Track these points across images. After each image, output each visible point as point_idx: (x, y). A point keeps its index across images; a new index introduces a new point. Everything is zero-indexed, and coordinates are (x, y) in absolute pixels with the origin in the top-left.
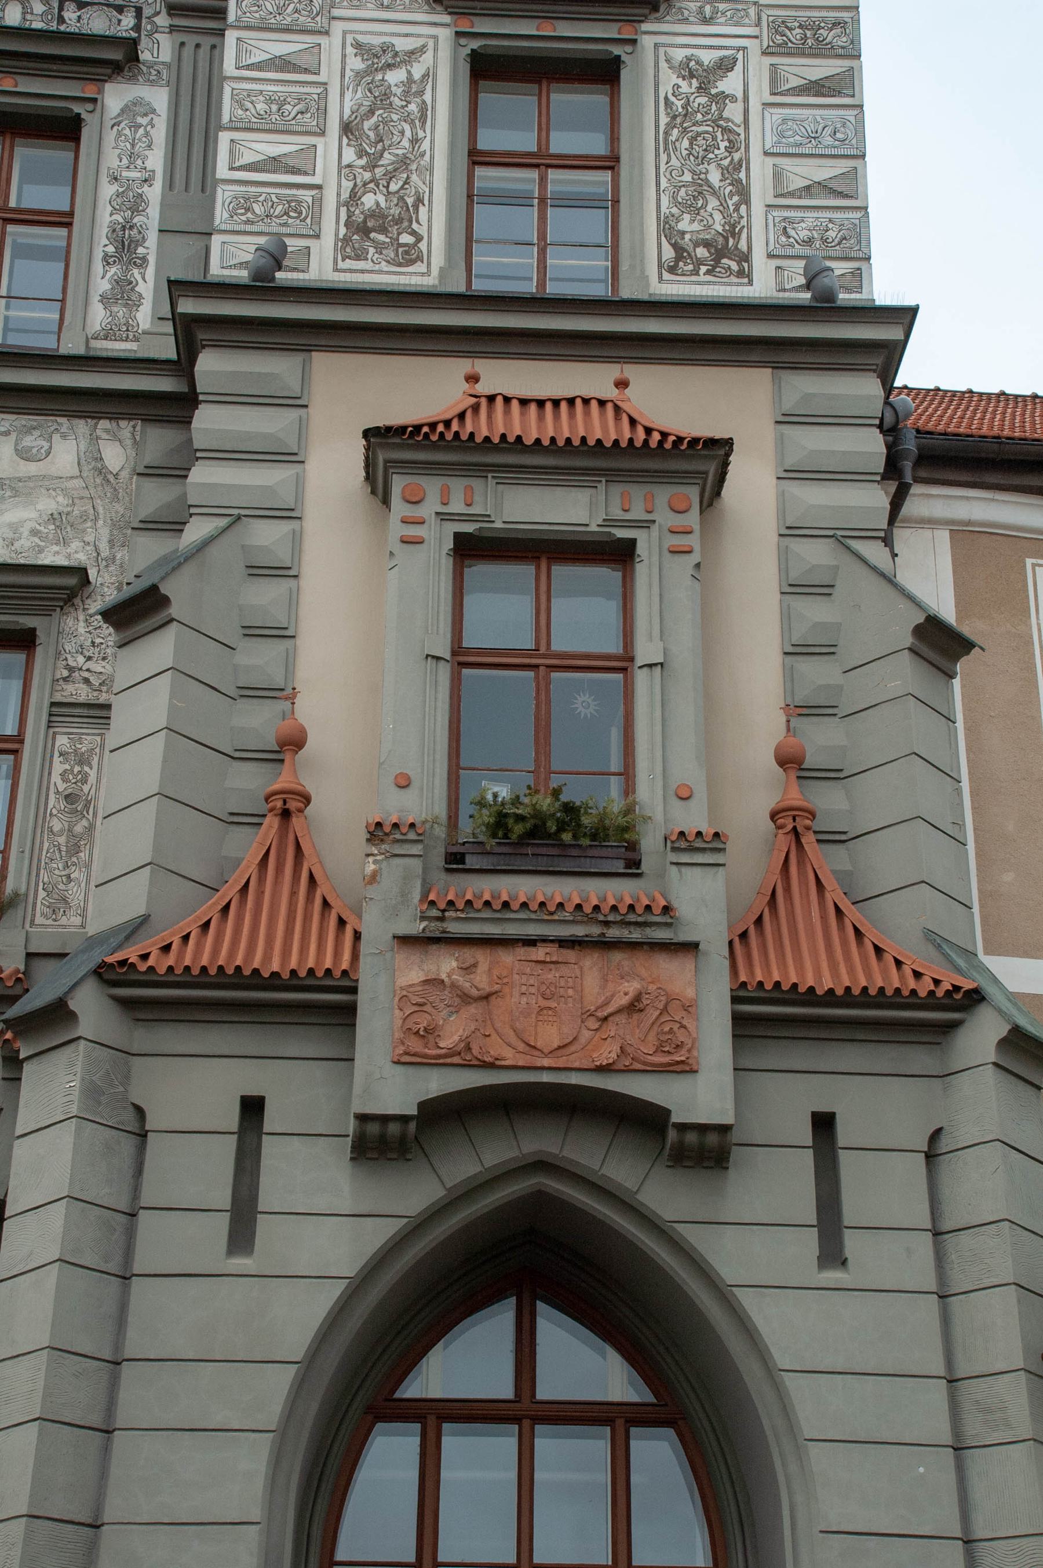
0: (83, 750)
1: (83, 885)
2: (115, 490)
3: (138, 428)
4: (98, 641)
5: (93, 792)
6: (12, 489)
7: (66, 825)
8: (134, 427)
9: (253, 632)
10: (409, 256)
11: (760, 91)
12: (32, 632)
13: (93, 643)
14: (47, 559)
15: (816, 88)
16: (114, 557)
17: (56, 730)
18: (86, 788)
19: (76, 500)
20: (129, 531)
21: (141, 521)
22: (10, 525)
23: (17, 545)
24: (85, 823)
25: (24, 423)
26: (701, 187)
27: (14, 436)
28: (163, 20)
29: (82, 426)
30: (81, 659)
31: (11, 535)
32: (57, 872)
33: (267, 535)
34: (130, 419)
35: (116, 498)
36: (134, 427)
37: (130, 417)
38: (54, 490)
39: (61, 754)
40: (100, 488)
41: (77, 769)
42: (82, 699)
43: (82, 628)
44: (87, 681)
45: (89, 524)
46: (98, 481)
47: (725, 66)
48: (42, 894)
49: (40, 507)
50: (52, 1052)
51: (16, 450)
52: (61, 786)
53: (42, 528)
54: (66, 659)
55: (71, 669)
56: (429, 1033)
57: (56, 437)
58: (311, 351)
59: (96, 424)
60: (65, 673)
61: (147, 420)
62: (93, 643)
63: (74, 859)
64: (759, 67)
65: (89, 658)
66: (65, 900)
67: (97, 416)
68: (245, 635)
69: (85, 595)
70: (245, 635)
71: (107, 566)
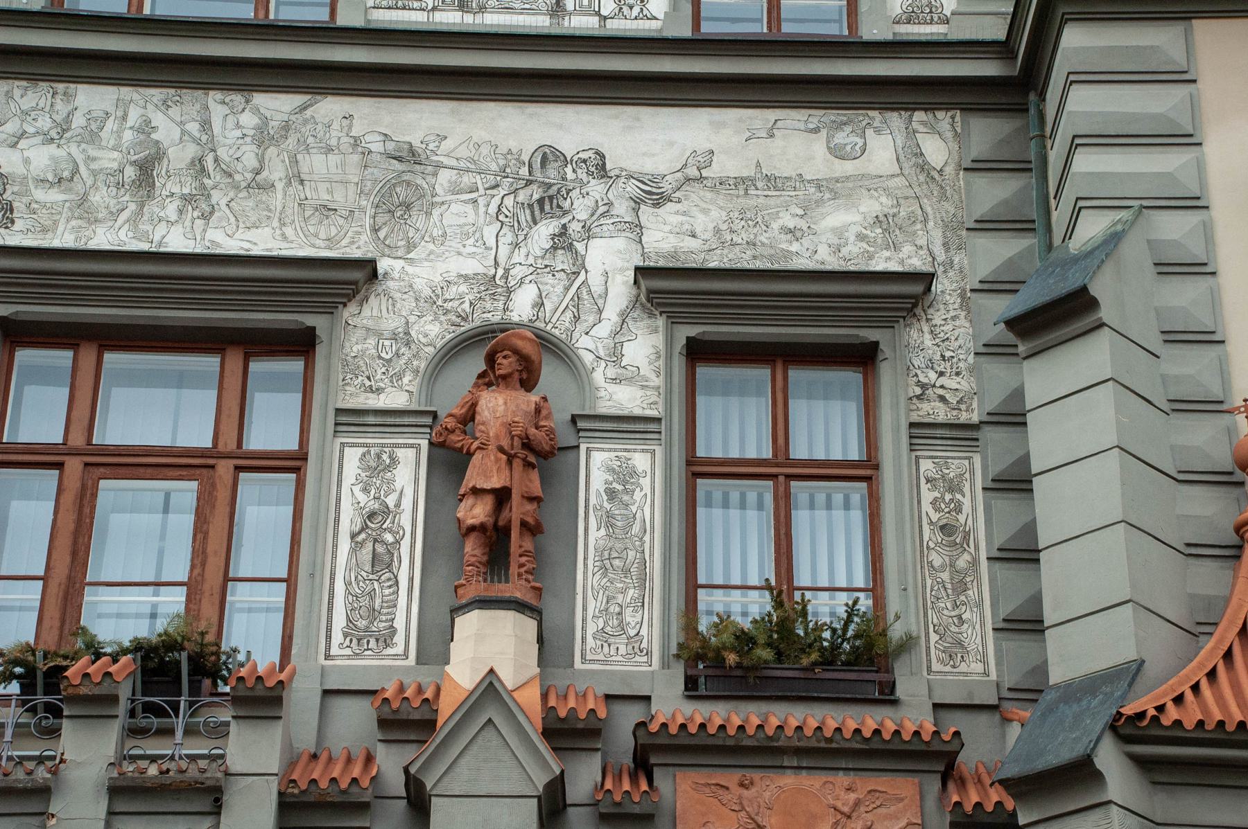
0: (952, 475)
1: (978, 627)
2: (942, 187)
3: (958, 118)
4: (948, 354)
5: (970, 522)
6: (831, 190)
7: (947, 559)
8: (953, 118)
9: (1174, 338)
12: (875, 345)
13: (943, 356)
14: (879, 265)
16: (952, 262)
17: (919, 453)
18: (962, 518)
19: (902, 201)
20: (964, 233)
21: (976, 221)
22: (834, 230)
23: (844, 251)
24: (966, 557)
25: (833, 118)
27: (824, 132)
29: (896, 120)
30: (933, 375)
31: (836, 241)
32: (945, 612)
33: (1173, 228)
34: (948, 109)
35: (943, 196)
36: (953, 118)
37: (947, 107)
38: (876, 190)
39: (928, 481)
40: (925, 186)
41: (948, 497)
42: (941, 418)
43: (928, 341)
44: (942, 399)
45: (919, 226)
46: (922, 178)
48: (934, 637)
49: (862, 209)
50: (1075, 816)
51: (829, 148)
52: (935, 517)
53: (868, 232)
54: (916, 375)
55: (924, 386)
57: (869, 132)
58: (1190, 18)
59: (911, 117)
60: (918, 391)
61: (967, 109)
62: (943, 356)
63: (963, 598)
65: (941, 374)
66: (960, 644)
67: (911, 108)
68: (1165, 341)
69: (927, 304)
70: (1165, 341)
71: (945, 272)
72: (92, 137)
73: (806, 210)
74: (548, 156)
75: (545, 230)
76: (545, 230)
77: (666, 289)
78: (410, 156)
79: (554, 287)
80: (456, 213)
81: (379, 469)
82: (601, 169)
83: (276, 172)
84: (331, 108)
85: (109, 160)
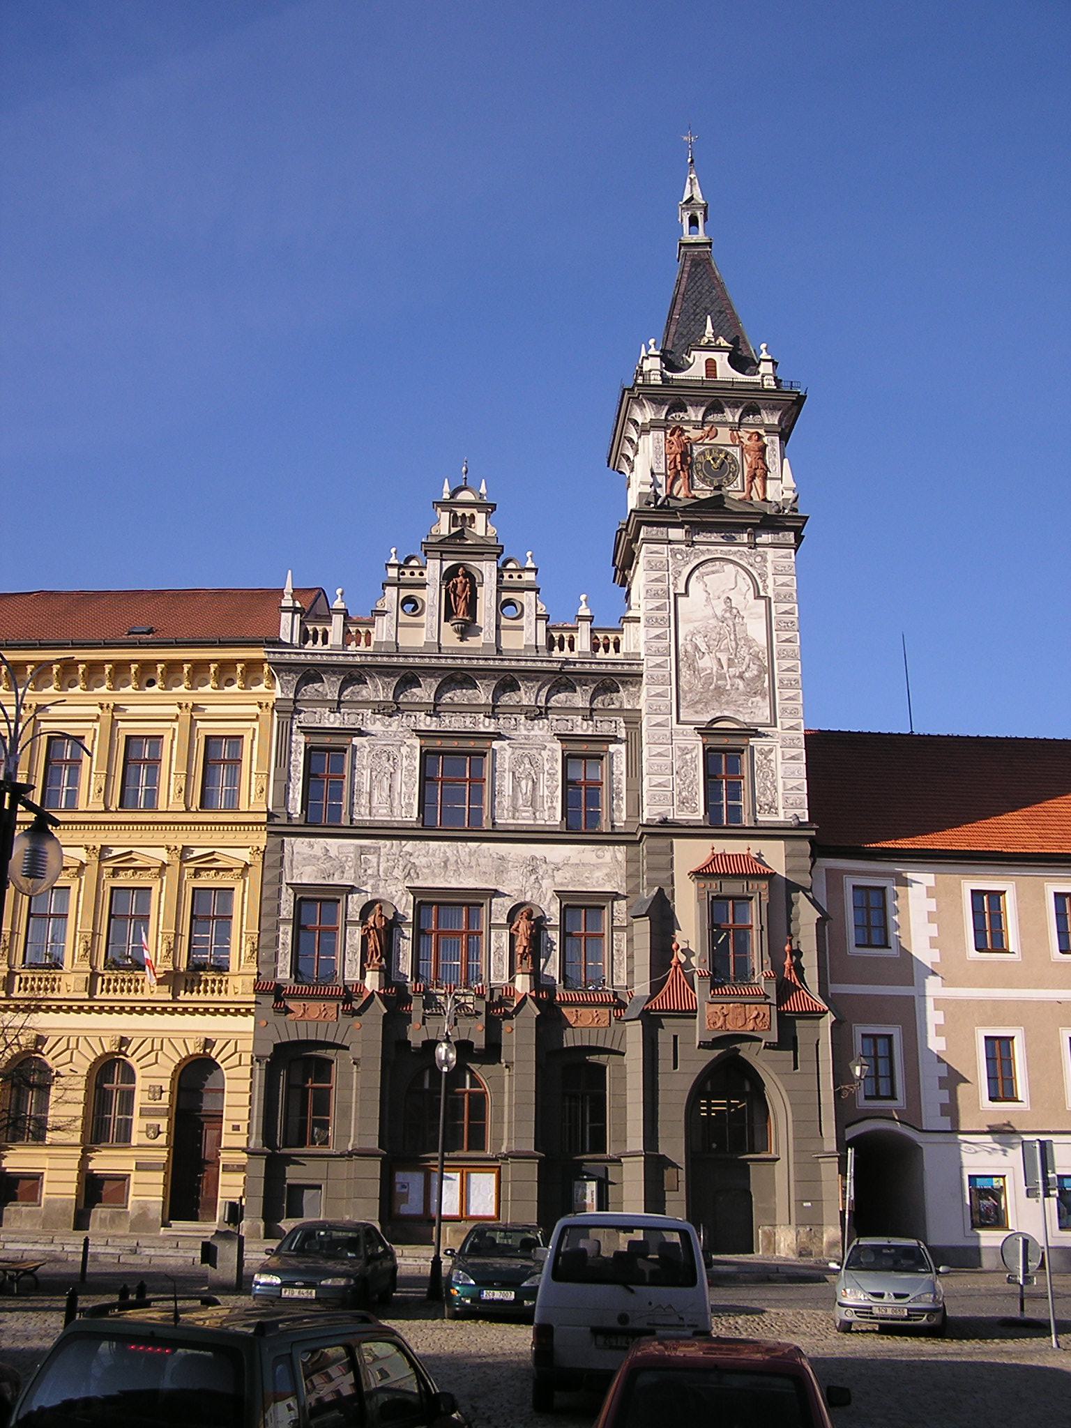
11: (780, 760)
15: (793, 758)
26: (766, 788)
28: (623, 725)
47: (771, 751)
56: (715, 1023)
64: (779, 751)
74: (533, 858)
75: (534, 877)
76: (534, 877)
78: (502, 858)
79: (535, 891)
80: (513, 873)
81: (499, 937)
83: (473, 863)
84: (485, 845)
85: (438, 861)
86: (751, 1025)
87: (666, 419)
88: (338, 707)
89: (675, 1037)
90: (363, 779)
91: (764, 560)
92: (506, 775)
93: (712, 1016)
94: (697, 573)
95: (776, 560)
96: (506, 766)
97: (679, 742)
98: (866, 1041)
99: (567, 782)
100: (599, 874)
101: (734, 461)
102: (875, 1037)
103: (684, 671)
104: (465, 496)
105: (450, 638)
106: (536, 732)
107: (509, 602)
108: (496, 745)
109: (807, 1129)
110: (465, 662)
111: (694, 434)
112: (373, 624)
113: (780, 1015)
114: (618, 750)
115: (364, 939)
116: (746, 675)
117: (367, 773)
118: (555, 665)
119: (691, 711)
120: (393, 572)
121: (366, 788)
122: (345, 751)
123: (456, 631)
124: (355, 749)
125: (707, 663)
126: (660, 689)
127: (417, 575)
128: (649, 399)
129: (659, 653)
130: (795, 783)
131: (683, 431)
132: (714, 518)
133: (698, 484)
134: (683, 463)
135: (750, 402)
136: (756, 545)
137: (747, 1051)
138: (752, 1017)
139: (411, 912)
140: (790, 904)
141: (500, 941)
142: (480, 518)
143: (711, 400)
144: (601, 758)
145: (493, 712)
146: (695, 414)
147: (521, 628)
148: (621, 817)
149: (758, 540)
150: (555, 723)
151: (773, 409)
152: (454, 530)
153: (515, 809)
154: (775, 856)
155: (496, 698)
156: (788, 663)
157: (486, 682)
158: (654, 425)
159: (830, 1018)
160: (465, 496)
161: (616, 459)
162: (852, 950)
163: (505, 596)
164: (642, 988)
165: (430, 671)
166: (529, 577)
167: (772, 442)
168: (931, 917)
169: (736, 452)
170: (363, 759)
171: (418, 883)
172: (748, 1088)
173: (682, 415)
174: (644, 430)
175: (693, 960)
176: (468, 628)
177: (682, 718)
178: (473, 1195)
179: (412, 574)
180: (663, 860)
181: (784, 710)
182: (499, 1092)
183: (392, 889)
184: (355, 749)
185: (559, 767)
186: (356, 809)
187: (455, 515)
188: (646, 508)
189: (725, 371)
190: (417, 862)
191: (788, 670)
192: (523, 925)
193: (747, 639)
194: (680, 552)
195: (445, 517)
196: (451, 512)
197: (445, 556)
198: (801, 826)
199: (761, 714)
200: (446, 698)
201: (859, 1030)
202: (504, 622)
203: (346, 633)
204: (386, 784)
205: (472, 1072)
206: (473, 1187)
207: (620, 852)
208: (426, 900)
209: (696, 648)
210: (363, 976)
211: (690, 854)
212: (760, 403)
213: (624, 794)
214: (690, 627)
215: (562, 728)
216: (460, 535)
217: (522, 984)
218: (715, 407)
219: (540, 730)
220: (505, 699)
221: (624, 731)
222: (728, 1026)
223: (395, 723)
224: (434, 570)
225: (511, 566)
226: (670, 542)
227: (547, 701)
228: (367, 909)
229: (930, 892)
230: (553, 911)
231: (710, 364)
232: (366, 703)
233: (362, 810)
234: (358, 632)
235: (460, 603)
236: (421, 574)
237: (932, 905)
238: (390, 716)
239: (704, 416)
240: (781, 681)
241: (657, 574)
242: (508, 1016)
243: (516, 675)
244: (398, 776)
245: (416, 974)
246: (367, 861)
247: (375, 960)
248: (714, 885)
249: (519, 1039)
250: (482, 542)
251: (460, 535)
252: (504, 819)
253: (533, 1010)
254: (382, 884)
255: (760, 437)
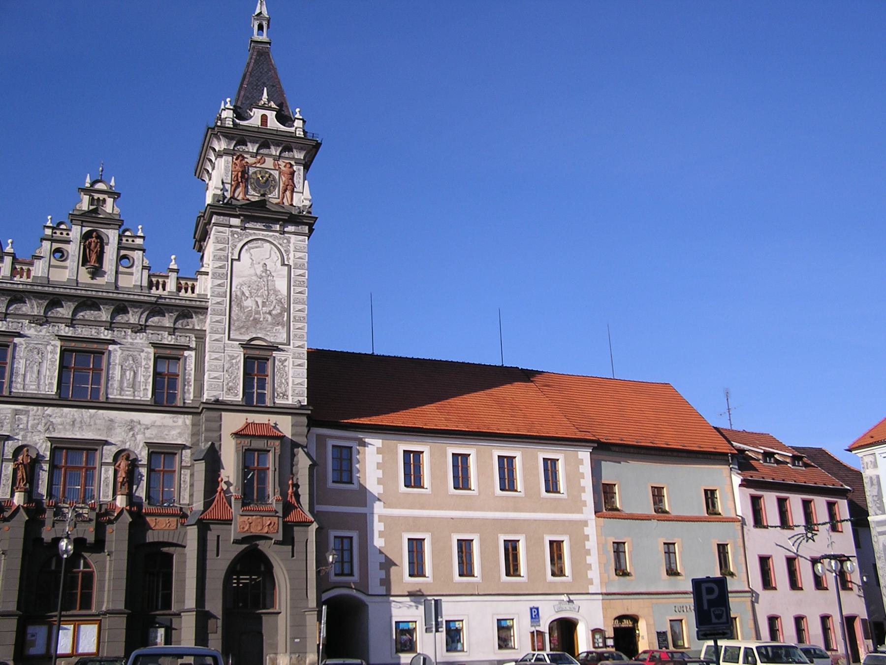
10: (237, 395)
11: (291, 366)
15: (299, 365)
26: (281, 383)
47: (286, 360)
64: (291, 360)
72: (66, 417)
73: (169, 431)
74: (132, 421)
77: (148, 444)
78: (111, 420)
80: (118, 430)
81: (107, 471)
82: (140, 424)
83: (92, 423)
84: (101, 412)
85: (68, 421)
86: (266, 530)
87: (234, 149)
88: (5, 318)
89: (218, 537)
90: (20, 365)
91: (289, 242)
92: (117, 367)
93: (242, 523)
94: (246, 247)
95: (296, 243)
96: (117, 362)
97: (229, 351)
98: (337, 540)
99: (156, 374)
100: (174, 432)
101: (274, 179)
102: (342, 538)
103: (234, 308)
104: (100, 186)
105: (84, 277)
106: (138, 341)
107: (125, 257)
108: (111, 347)
109: (298, 594)
110: (94, 293)
111: (250, 160)
112: (32, 264)
113: (285, 524)
114: (190, 355)
115: (15, 471)
116: (274, 312)
117: (23, 362)
118: (152, 299)
119: (238, 333)
120: (48, 232)
121: (22, 371)
122: (8, 346)
123: (89, 273)
124: (15, 345)
125: (249, 303)
126: (218, 318)
127: (65, 235)
128: (224, 136)
129: (219, 295)
130: (300, 381)
131: (244, 158)
132: (260, 214)
133: (251, 192)
134: (242, 177)
135: (287, 144)
136: (284, 233)
137: (263, 546)
138: (266, 525)
139: (48, 453)
140: (293, 455)
141: (108, 474)
142: (110, 201)
143: (263, 140)
144: (179, 359)
145: (110, 326)
146: (252, 148)
147: (132, 274)
148: (190, 397)
149: (286, 229)
150: (150, 336)
151: (301, 149)
152: (91, 207)
153: (122, 389)
154: (285, 425)
155: (112, 317)
156: (300, 307)
157: (107, 307)
158: (226, 152)
159: (315, 526)
160: (100, 186)
161: (200, 171)
162: (330, 484)
163: (123, 252)
164: (198, 505)
165: (70, 298)
166: (139, 241)
167: (299, 170)
168: (379, 466)
169: (276, 174)
170: (21, 352)
171: (54, 435)
172: (263, 569)
173: (244, 147)
174: (219, 155)
175: (232, 489)
176: (97, 272)
177: (232, 337)
178: (81, 637)
179: (62, 234)
180: (215, 425)
181: (295, 335)
182: (102, 571)
183: (36, 438)
184: (15, 345)
185: (151, 363)
186: (14, 385)
187: (93, 199)
188: (217, 204)
189: (273, 123)
190: (54, 420)
191: (299, 311)
192: (123, 464)
193: (276, 292)
194: (237, 233)
195: (86, 199)
196: (90, 195)
197: (84, 224)
198: (302, 407)
199: (282, 337)
200: (80, 315)
201: (333, 533)
202: (121, 269)
203: (14, 269)
204: (36, 369)
205: (85, 559)
206: (82, 633)
207: (188, 419)
208: (59, 446)
209: (243, 293)
210: (12, 495)
211: (232, 422)
212: (293, 145)
213: (192, 383)
214: (240, 280)
215: (155, 339)
216: (96, 211)
217: (121, 501)
218: (265, 145)
219: (141, 339)
220: (120, 318)
221: (194, 343)
222: (252, 530)
223: (44, 330)
224: (76, 232)
225: (127, 233)
226: (231, 226)
227: (146, 321)
228: (18, 451)
229: (379, 451)
230: (143, 455)
231: (264, 118)
232: (25, 316)
233: (18, 386)
234: (22, 269)
235: (93, 255)
236: (68, 234)
237: (379, 458)
238: (41, 325)
239: (258, 150)
240: (294, 317)
241: (222, 246)
242: (111, 522)
243: (126, 304)
244: (45, 365)
245: (50, 494)
246: (19, 419)
247: (22, 485)
248: (246, 442)
249: (117, 537)
250: (109, 217)
251: (96, 211)
252: (114, 395)
253: (127, 518)
254: (29, 434)
255: (291, 166)
